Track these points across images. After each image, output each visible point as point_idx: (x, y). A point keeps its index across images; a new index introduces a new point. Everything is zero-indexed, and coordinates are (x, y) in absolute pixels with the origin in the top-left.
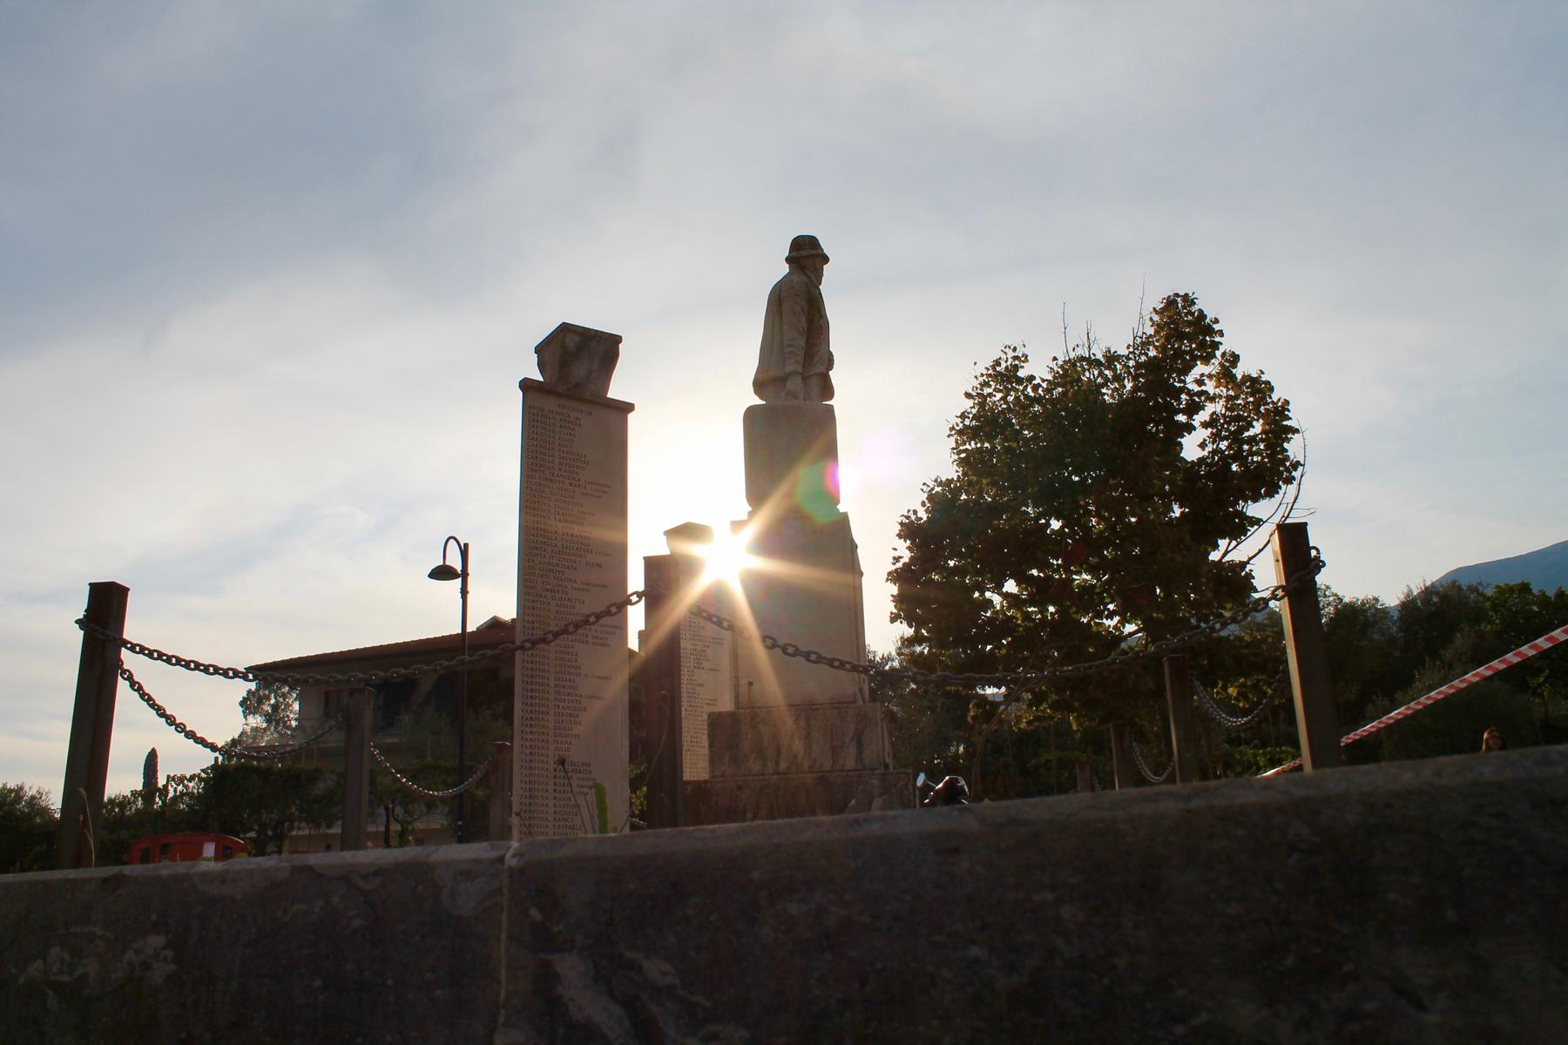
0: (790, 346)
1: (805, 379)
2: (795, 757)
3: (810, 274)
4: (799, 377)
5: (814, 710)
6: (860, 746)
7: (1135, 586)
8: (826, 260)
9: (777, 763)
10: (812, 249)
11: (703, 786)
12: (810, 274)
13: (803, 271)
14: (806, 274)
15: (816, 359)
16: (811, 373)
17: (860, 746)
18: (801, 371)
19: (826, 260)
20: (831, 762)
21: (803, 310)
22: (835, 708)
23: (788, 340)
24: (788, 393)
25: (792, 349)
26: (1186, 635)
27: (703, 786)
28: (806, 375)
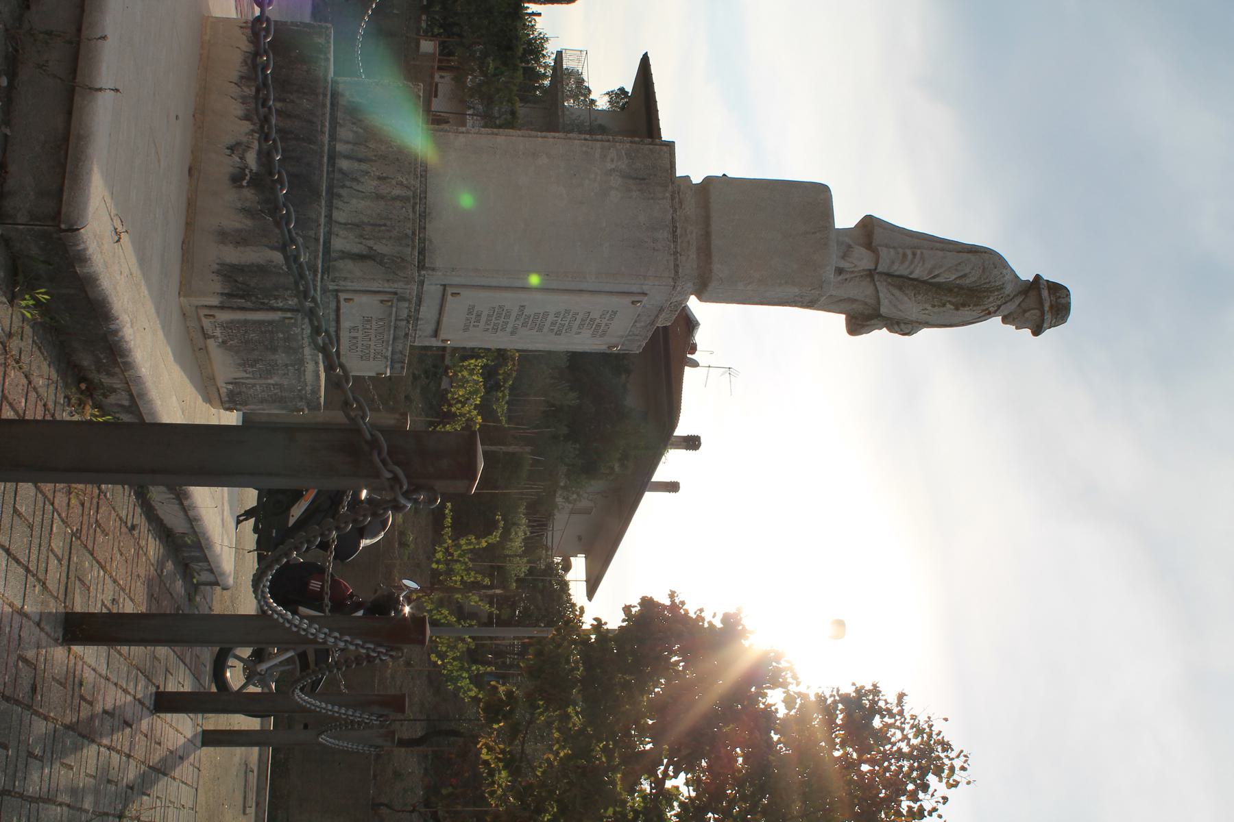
0: (914, 254)
1: (871, 274)
2: (355, 180)
3: (1017, 301)
4: (872, 267)
5: (414, 208)
6: (361, 257)
7: (530, 577)
8: (1037, 332)
9: (347, 157)
10: (1051, 307)
11: (322, 56)
12: (1017, 301)
13: (1020, 293)
14: (1015, 296)
15: (897, 293)
16: (877, 283)
17: (361, 257)
18: (880, 269)
19: (1037, 332)
20: (343, 221)
21: (965, 276)
22: (414, 233)
23: (922, 253)
24: (850, 246)
25: (910, 257)
26: (360, 79)
27: (322, 56)
28: (876, 277)
